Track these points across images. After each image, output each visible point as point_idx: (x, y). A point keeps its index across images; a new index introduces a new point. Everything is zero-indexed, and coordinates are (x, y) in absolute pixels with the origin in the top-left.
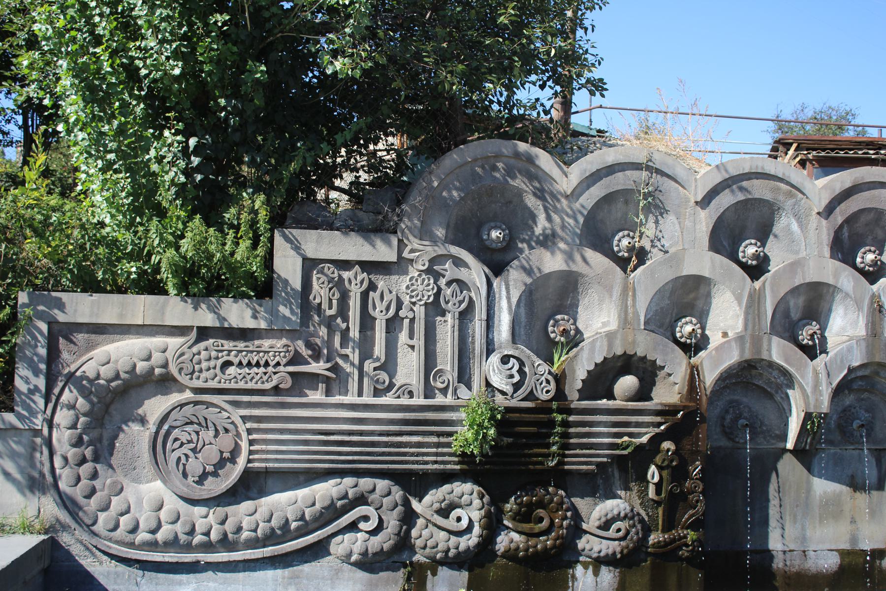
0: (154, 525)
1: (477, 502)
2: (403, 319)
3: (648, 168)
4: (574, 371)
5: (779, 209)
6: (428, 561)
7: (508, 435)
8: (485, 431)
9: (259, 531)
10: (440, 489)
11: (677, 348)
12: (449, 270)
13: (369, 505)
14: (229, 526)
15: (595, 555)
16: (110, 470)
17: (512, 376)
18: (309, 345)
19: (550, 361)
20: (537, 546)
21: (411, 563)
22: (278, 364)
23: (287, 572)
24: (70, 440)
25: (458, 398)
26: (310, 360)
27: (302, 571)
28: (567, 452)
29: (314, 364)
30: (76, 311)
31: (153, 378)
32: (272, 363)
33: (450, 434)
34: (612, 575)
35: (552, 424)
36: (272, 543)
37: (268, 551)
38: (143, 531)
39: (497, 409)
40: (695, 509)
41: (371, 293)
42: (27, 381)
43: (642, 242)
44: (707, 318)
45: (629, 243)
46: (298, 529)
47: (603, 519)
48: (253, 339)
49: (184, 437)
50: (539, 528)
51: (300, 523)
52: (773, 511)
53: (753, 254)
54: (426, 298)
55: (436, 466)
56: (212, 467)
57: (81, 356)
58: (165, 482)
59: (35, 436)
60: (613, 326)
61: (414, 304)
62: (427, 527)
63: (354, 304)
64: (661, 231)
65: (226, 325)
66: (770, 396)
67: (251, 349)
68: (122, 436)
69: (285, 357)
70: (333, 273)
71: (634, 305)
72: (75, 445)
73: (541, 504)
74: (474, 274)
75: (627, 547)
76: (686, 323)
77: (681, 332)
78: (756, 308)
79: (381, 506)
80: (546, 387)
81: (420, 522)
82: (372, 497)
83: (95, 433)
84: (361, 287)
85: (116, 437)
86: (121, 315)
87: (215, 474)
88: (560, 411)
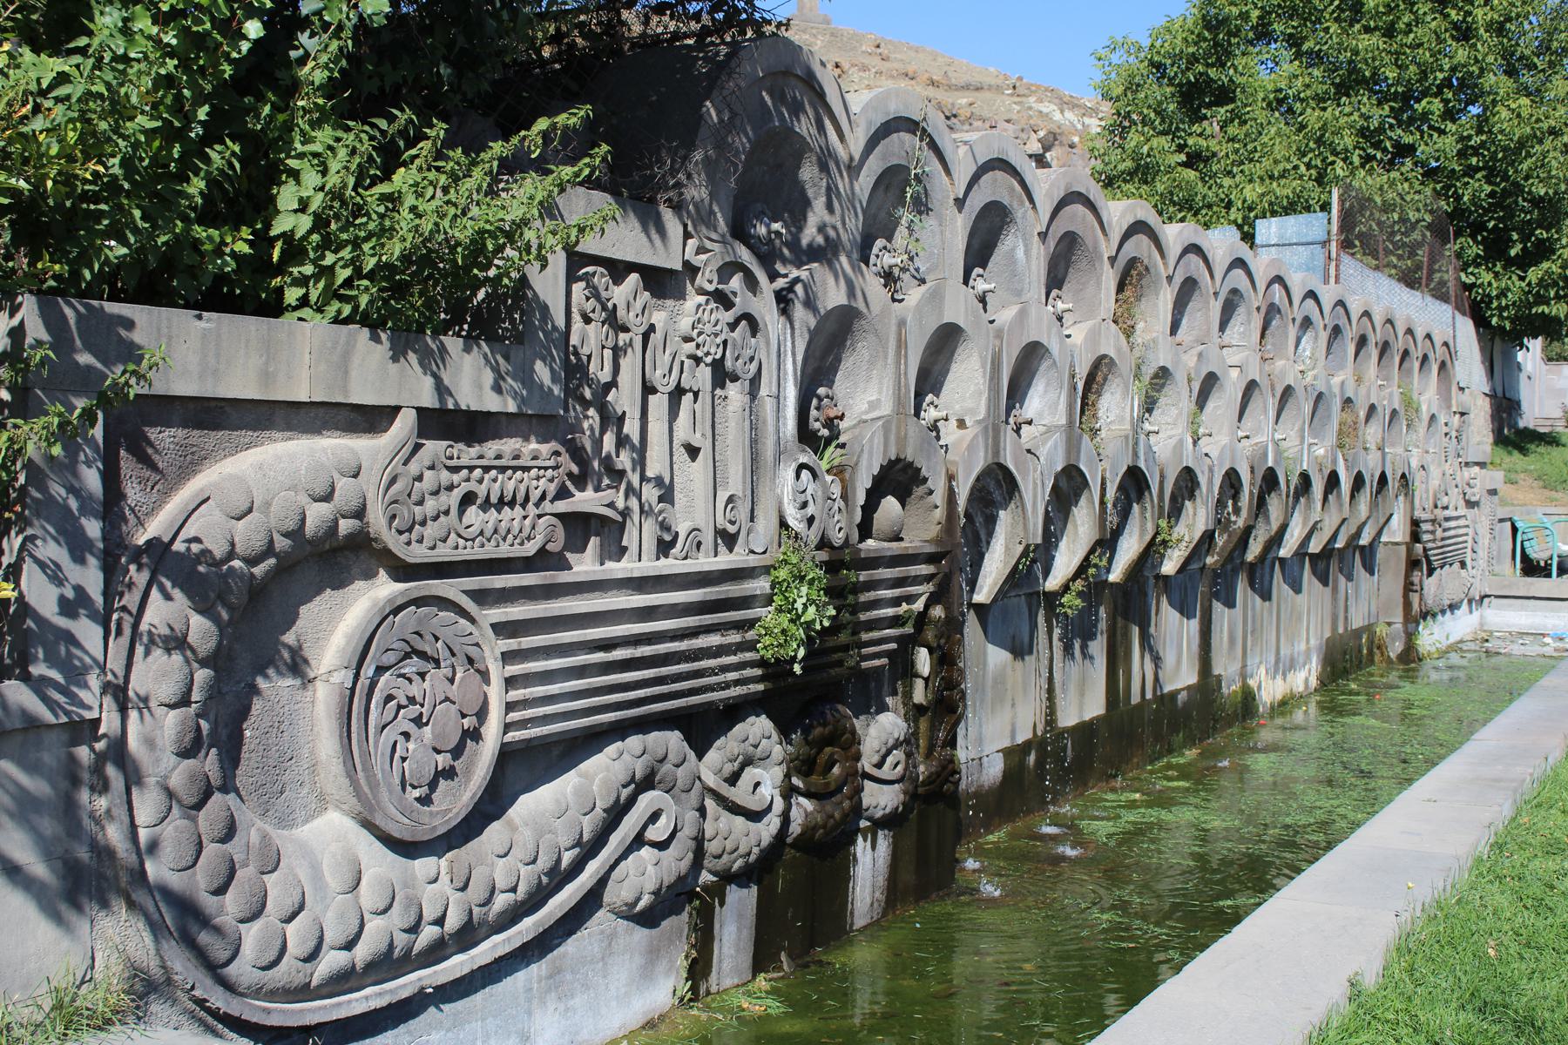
1: (778, 751)
14: (476, 892)
15: (879, 814)
24: (179, 741)
25: (752, 552)
27: (564, 955)
32: (535, 495)
33: (750, 624)
37: (528, 927)
42: (55, 575)
47: (884, 750)
49: (402, 691)
51: (577, 850)
57: (167, 494)
67: (503, 462)
68: (257, 705)
69: (551, 480)
71: (906, 374)
72: (186, 753)
73: (830, 740)
85: (244, 712)
86: (266, 377)
87: (449, 773)
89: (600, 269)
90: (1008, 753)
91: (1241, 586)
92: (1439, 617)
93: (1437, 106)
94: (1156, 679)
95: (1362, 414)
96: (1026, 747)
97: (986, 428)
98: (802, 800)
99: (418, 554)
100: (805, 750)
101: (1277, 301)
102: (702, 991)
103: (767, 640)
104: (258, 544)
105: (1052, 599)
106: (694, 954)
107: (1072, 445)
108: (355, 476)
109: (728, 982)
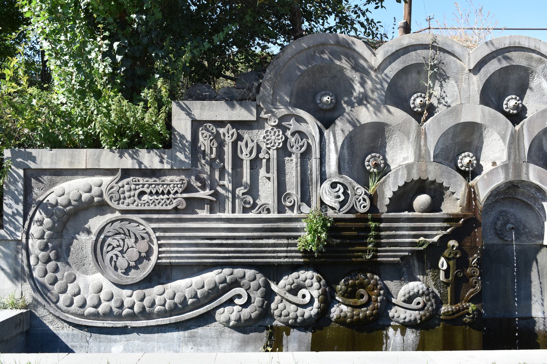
0: (96, 302)
1: (316, 285)
2: (262, 159)
3: (434, 47)
4: (383, 193)
5: (532, 72)
6: (283, 325)
7: (336, 238)
8: (319, 235)
9: (167, 305)
10: (290, 276)
11: (458, 174)
12: (293, 125)
13: (241, 287)
14: (146, 303)
15: (402, 321)
16: (67, 266)
17: (338, 197)
18: (198, 179)
19: (366, 185)
20: (359, 314)
21: (272, 327)
22: (176, 192)
23: (187, 333)
24: (39, 246)
25: (302, 213)
26: (199, 189)
27: (197, 332)
28: (379, 249)
29: (202, 192)
30: (41, 161)
31: (93, 204)
32: (172, 192)
33: (296, 238)
34: (414, 335)
35: (368, 229)
36: (178, 313)
37: (173, 319)
38: (90, 307)
39: (328, 220)
40: (474, 288)
41: (239, 142)
42: (10, 207)
43: (431, 101)
44: (481, 153)
45: (421, 101)
46: (193, 303)
47: (407, 296)
48: (158, 177)
49: (115, 243)
50: (361, 302)
51: (194, 300)
52: (535, 289)
53: (514, 106)
54: (277, 144)
55: (286, 260)
56: (134, 263)
57: (46, 191)
58: (103, 273)
59: (18, 244)
60: (411, 159)
61: (269, 149)
62: (282, 301)
63: (228, 150)
64: (444, 92)
66: (529, 207)
67: (158, 182)
69: (181, 187)
70: (213, 129)
71: (426, 145)
72: (42, 250)
73: (362, 285)
74: (311, 127)
75: (425, 315)
76: (465, 157)
77: (461, 163)
78: (517, 144)
79: (250, 288)
80: (363, 203)
81: (277, 298)
82: (243, 282)
83: (56, 242)
84: (232, 138)
85: (71, 244)
86: (71, 163)
87: (136, 267)
88: (374, 220)
99: (123, 207)
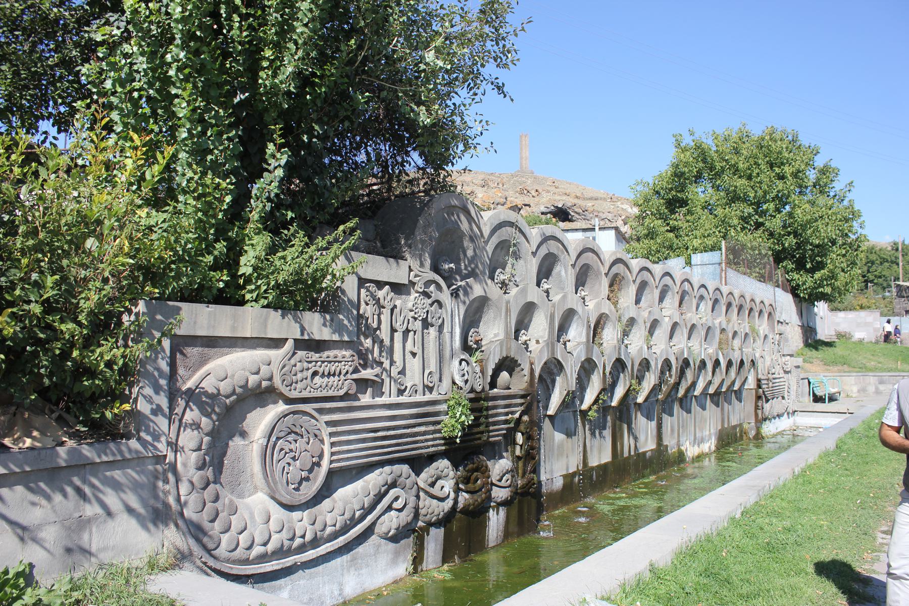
1: (452, 474)
9: (338, 525)
14: (318, 526)
15: (499, 500)
24: (197, 464)
26: (359, 367)
27: (358, 553)
29: (363, 372)
30: (195, 323)
32: (344, 372)
33: (439, 423)
37: (341, 541)
42: (149, 400)
51: (362, 511)
57: (195, 372)
65: (306, 337)
69: (351, 366)
73: (477, 470)
81: (422, 494)
85: (224, 454)
86: (234, 328)
87: (307, 479)
89: (372, 285)
90: (565, 477)
91: (676, 408)
92: (773, 420)
93: (772, 206)
94: (636, 446)
95: (730, 335)
96: (573, 475)
97: (548, 343)
98: (463, 493)
99: (294, 394)
100: (465, 473)
101: (686, 289)
102: (419, 570)
103: (446, 429)
104: (229, 390)
105: (584, 414)
106: (415, 554)
107: (589, 350)
108: (269, 365)
109: (431, 567)
